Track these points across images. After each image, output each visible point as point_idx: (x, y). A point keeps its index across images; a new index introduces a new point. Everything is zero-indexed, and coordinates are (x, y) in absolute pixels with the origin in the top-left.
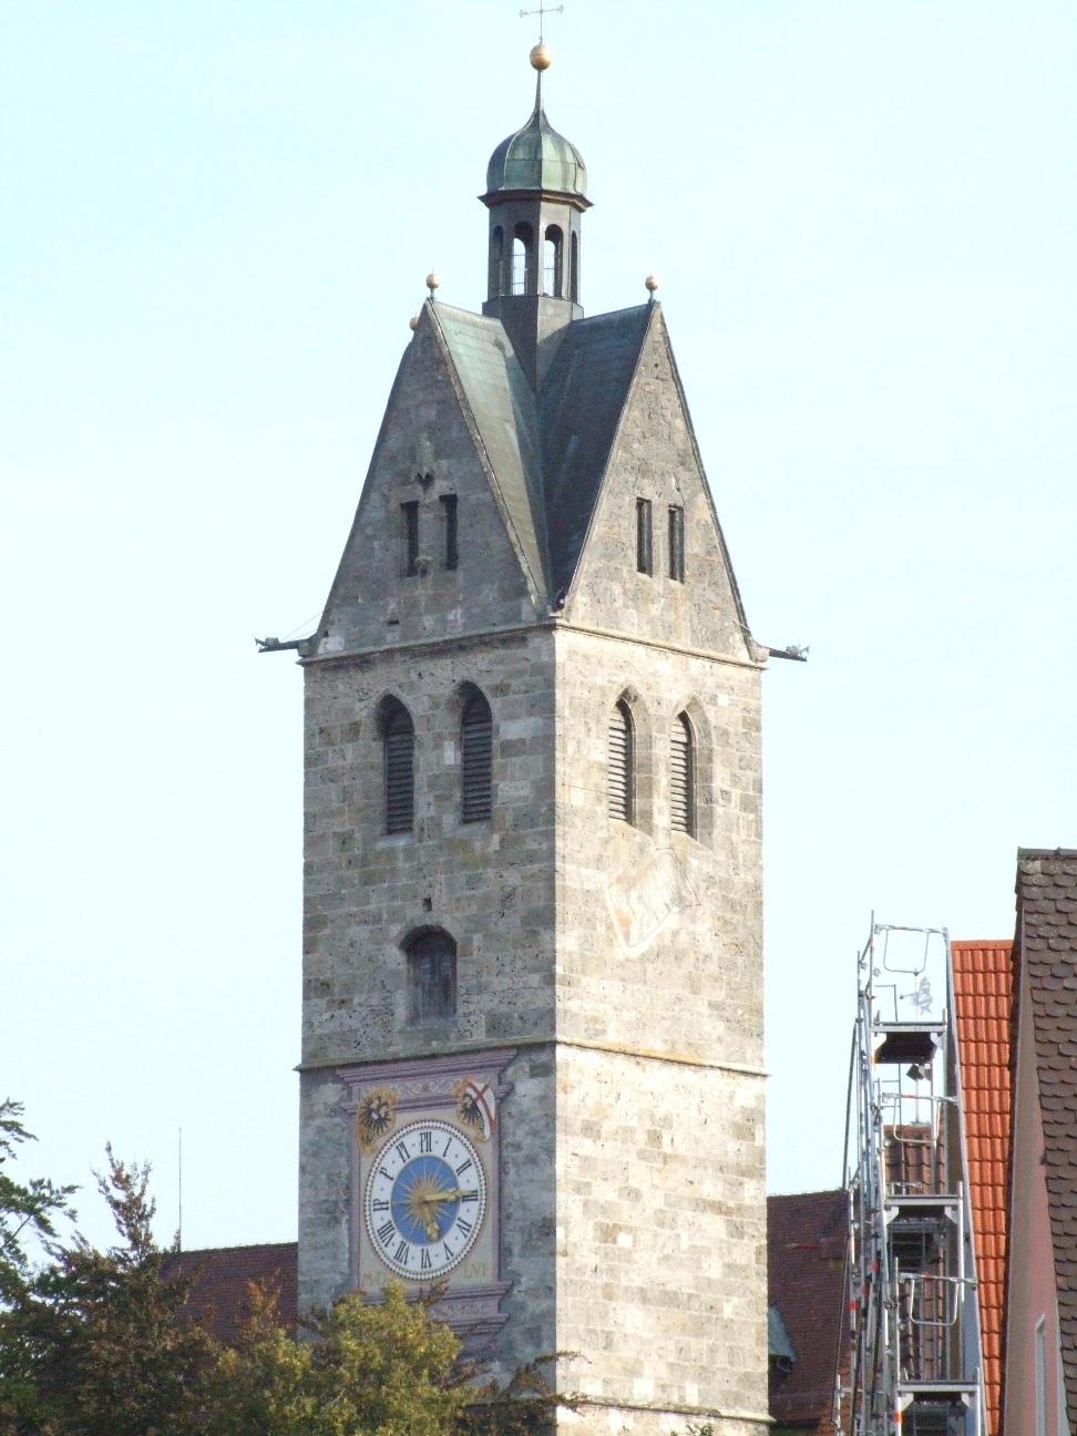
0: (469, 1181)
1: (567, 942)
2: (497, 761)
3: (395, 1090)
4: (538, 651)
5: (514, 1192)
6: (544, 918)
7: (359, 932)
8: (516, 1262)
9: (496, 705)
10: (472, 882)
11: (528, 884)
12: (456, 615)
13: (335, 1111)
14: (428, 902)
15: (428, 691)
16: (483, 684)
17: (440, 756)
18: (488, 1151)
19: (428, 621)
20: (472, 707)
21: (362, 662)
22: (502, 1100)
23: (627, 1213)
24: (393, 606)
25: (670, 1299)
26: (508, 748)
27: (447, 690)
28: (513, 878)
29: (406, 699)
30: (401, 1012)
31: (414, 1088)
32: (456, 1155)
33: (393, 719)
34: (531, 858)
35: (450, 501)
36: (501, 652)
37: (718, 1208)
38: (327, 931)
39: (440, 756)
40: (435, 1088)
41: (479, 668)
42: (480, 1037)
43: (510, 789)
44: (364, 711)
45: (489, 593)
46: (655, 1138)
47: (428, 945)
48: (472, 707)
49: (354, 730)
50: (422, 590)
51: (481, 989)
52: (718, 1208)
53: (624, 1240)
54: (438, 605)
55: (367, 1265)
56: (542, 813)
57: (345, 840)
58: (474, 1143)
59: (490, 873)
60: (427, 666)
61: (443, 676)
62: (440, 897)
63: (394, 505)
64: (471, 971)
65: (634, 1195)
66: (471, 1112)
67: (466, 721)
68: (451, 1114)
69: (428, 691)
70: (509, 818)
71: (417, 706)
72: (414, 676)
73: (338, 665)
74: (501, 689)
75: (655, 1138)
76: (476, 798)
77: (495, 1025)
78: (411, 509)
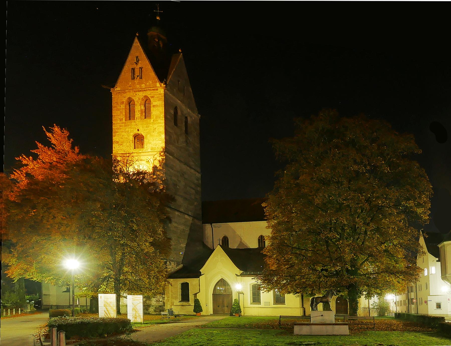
2: (152, 108)
9: (152, 100)
12: (143, 86)
14: (138, 130)
19: (138, 86)
24: (130, 83)
26: (154, 106)
35: (141, 68)
44: (125, 100)
49: (123, 102)
50: (136, 81)
54: (140, 83)
59: (151, 125)
60: (137, 93)
61: (141, 95)
64: (147, 140)
71: (136, 99)
72: (135, 94)
74: (152, 97)
77: (152, 149)
78: (133, 70)
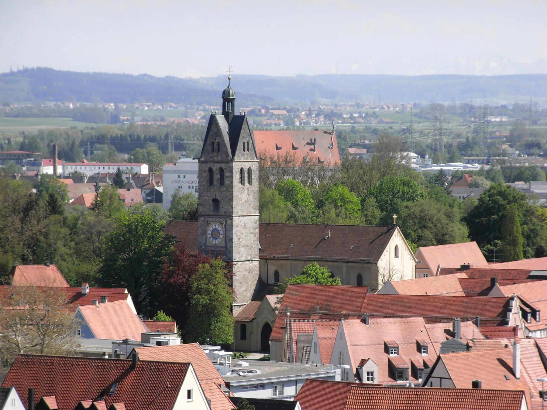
0: (221, 232)
1: (234, 203)
3: (211, 219)
5: (227, 234)
6: (231, 200)
8: (227, 243)
9: (225, 171)
10: (222, 194)
12: (219, 158)
13: (203, 221)
15: (216, 167)
17: (217, 176)
18: (224, 229)
19: (216, 158)
20: (221, 170)
21: (207, 162)
22: (226, 222)
23: (242, 236)
25: (247, 246)
26: (226, 176)
27: (218, 168)
29: (213, 168)
30: (212, 209)
31: (214, 219)
32: (220, 229)
34: (229, 191)
35: (218, 143)
37: (253, 233)
39: (217, 176)
40: (217, 220)
41: (223, 165)
42: (223, 214)
43: (227, 182)
44: (207, 169)
45: (224, 156)
46: (245, 225)
47: (216, 202)
48: (221, 170)
49: (205, 171)
50: (215, 154)
51: (223, 208)
52: (253, 233)
53: (241, 240)
54: (217, 156)
55: (208, 242)
56: (231, 186)
57: (204, 186)
58: (222, 228)
60: (215, 164)
62: (217, 195)
65: (242, 233)
66: (222, 223)
67: (220, 171)
68: (219, 223)
73: (203, 162)
74: (226, 169)
75: (245, 225)
76: (222, 182)
77: (225, 212)
78: (213, 143)
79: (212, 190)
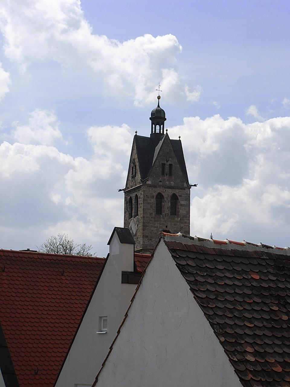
4: (187, 191)
7: (152, 228)
9: (179, 198)
11: (185, 227)
14: (166, 227)
15: (167, 193)
16: (177, 194)
17: (167, 204)
19: (167, 183)
20: (174, 198)
21: (155, 187)
26: (181, 205)
28: (182, 225)
33: (160, 197)
34: (186, 223)
35: (171, 165)
36: (181, 190)
38: (148, 228)
39: (167, 204)
44: (155, 194)
48: (174, 198)
57: (151, 214)
60: (167, 189)
61: (170, 192)
62: (169, 226)
63: (161, 163)
69: (167, 193)
70: (182, 216)
71: (165, 195)
74: (180, 196)
76: (174, 211)
78: (164, 165)
79: (162, 219)
